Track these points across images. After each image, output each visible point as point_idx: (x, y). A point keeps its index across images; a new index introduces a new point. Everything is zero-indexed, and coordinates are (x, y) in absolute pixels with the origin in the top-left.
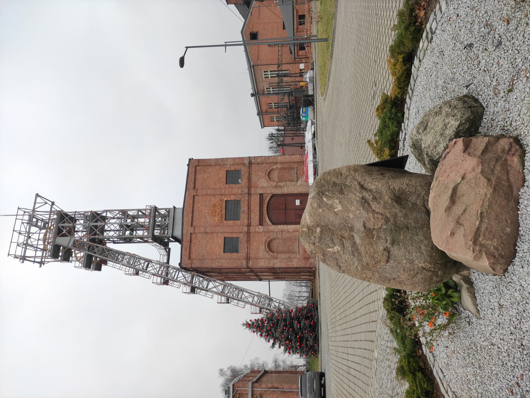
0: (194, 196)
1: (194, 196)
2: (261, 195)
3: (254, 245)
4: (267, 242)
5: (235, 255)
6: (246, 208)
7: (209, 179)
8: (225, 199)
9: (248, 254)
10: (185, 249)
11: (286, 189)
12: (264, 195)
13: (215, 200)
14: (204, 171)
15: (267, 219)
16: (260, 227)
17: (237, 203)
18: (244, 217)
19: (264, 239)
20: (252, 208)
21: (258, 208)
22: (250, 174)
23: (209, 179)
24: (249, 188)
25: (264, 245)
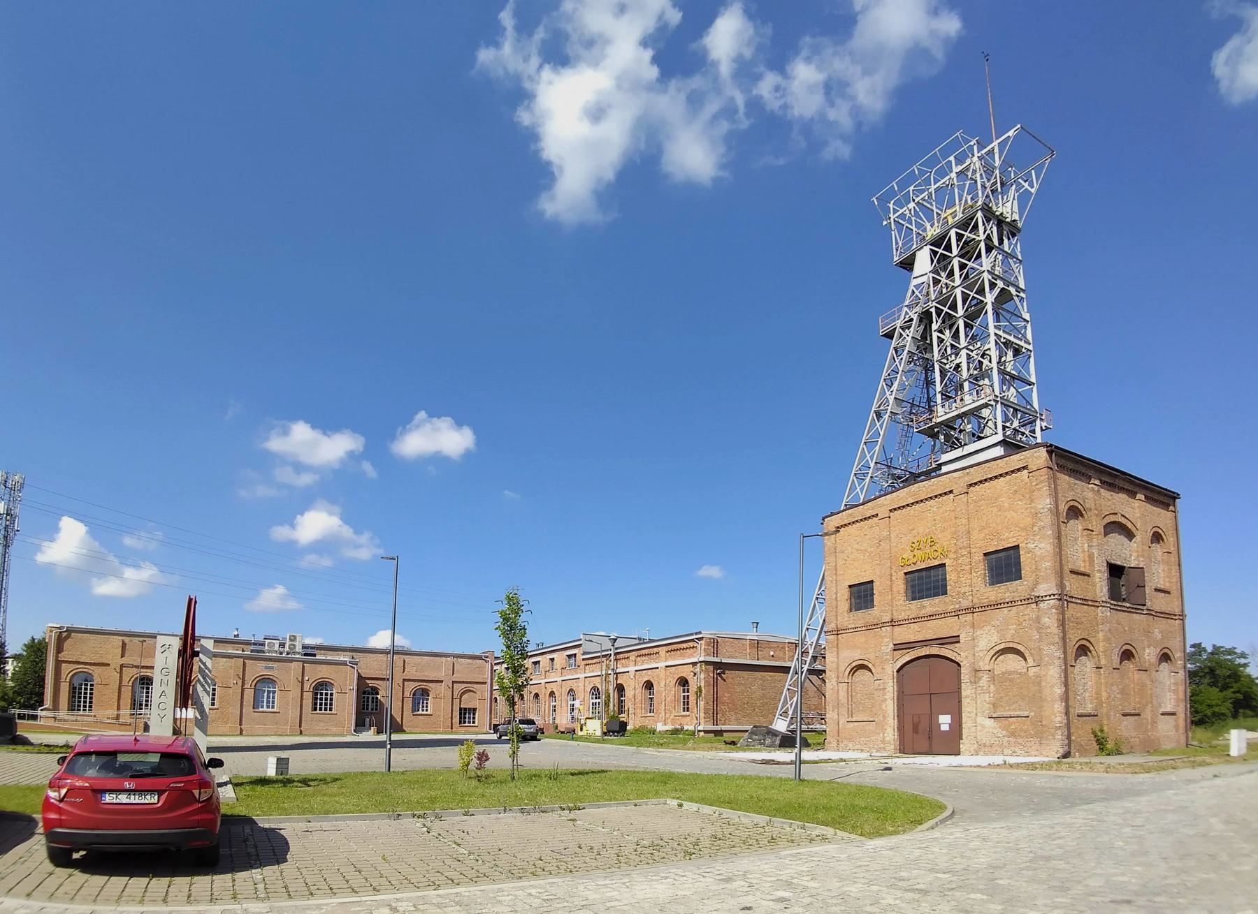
0: (951, 492)
1: (951, 492)
2: (954, 640)
3: (860, 638)
5: (844, 605)
7: (995, 510)
9: (846, 630)
11: (968, 692)
13: (945, 540)
15: (907, 658)
16: (891, 645)
17: (939, 589)
18: (915, 608)
19: (872, 657)
22: (1010, 604)
23: (995, 510)
24: (972, 610)
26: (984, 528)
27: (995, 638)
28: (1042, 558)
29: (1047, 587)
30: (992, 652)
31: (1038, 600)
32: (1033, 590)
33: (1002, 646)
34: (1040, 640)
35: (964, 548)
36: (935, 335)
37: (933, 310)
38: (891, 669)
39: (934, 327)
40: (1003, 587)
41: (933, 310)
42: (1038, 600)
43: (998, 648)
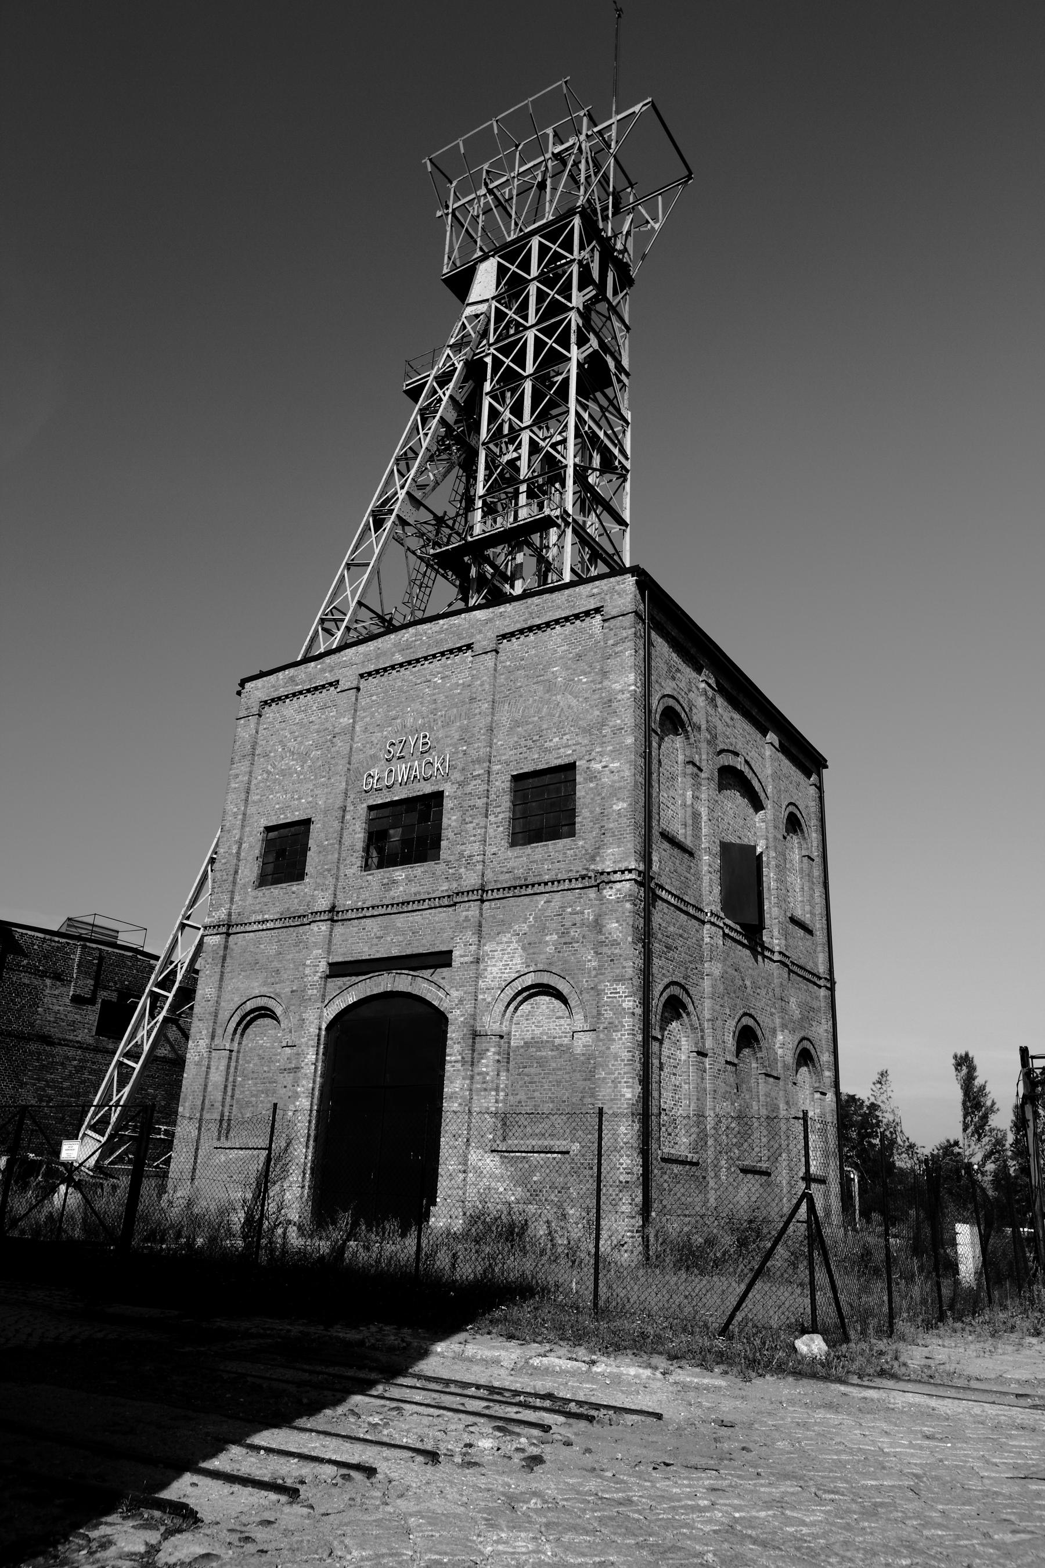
0: (469, 647)
4: (271, 1004)
6: (399, 893)
8: (448, 789)
10: (292, 679)
12: (445, 971)
14: (579, 657)
15: (351, 998)
16: (323, 967)
20: (400, 921)
21: (395, 952)
24: (482, 894)
25: (264, 990)
26: (517, 724)
27: (518, 963)
28: (615, 793)
29: (619, 854)
30: (510, 992)
31: (600, 881)
32: (593, 859)
33: (529, 980)
34: (600, 970)
35: (479, 761)
36: (487, 401)
37: (488, 360)
38: (317, 1018)
39: (487, 387)
40: (539, 851)
41: (488, 360)
42: (600, 881)
43: (518, 985)
